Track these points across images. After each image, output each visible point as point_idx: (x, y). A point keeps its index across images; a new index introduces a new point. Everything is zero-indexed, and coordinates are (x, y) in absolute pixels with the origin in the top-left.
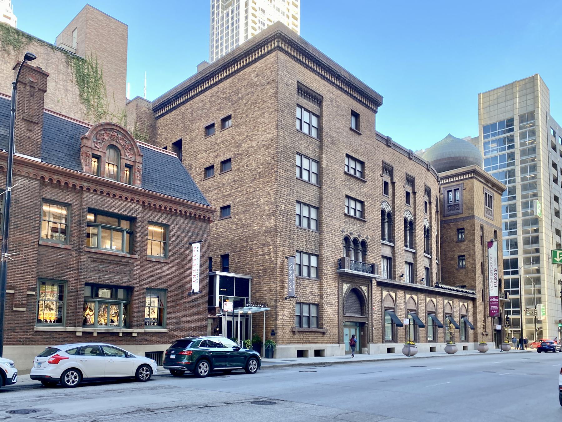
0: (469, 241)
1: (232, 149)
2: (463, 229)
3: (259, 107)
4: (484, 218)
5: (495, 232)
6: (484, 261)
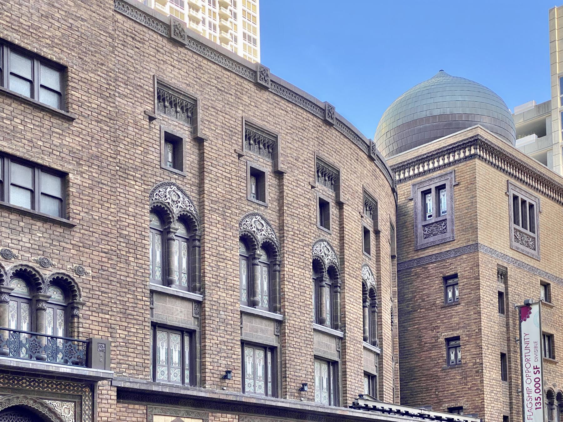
5: (546, 286)
6: (509, 351)
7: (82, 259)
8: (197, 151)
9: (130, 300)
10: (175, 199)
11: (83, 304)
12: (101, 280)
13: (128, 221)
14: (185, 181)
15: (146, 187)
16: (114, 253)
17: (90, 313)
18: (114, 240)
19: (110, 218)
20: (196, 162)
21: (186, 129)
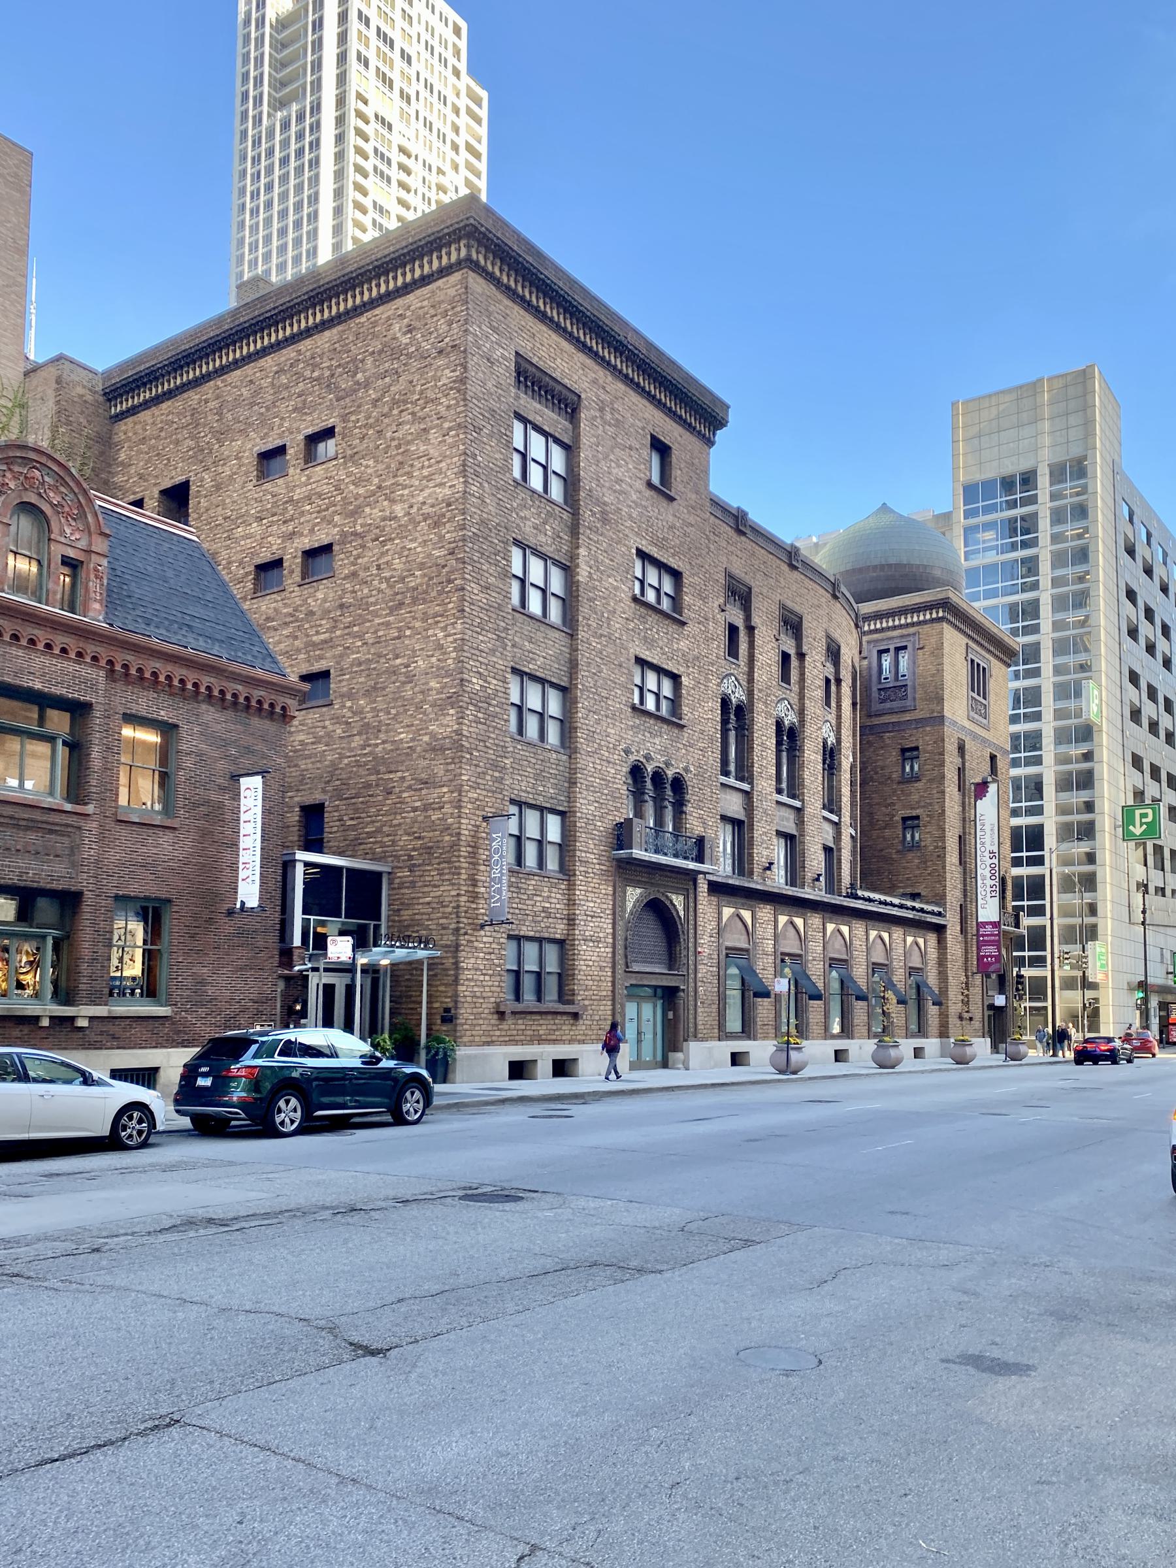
0: (931, 781)
1: (336, 518)
2: (916, 748)
3: (413, 414)
4: (967, 724)
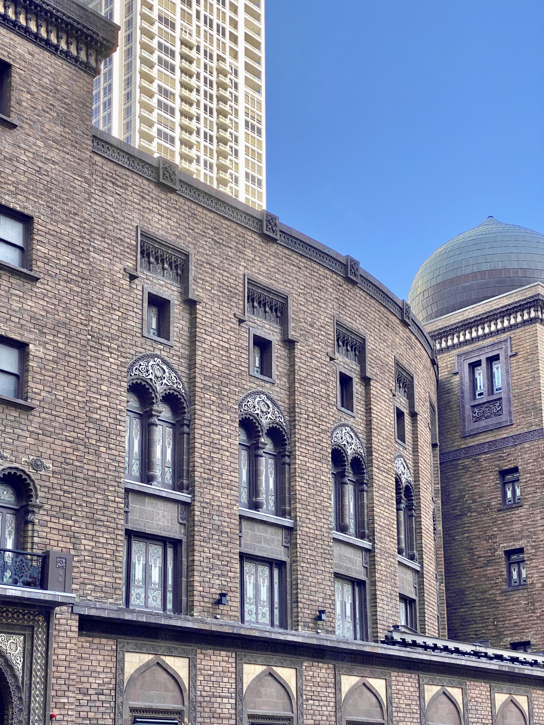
0: (532, 505)
2: (515, 470)
7: (41, 449)
8: (188, 316)
9: (100, 502)
10: (159, 374)
11: (40, 507)
12: (64, 476)
13: (99, 402)
14: (172, 352)
15: (123, 360)
16: (81, 442)
17: (48, 518)
18: (82, 426)
19: (78, 398)
20: (186, 329)
21: (175, 289)
